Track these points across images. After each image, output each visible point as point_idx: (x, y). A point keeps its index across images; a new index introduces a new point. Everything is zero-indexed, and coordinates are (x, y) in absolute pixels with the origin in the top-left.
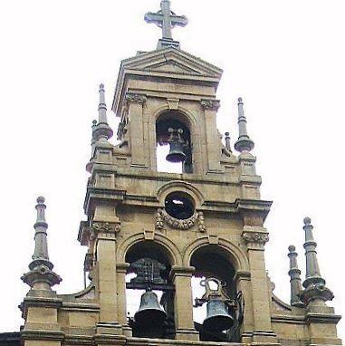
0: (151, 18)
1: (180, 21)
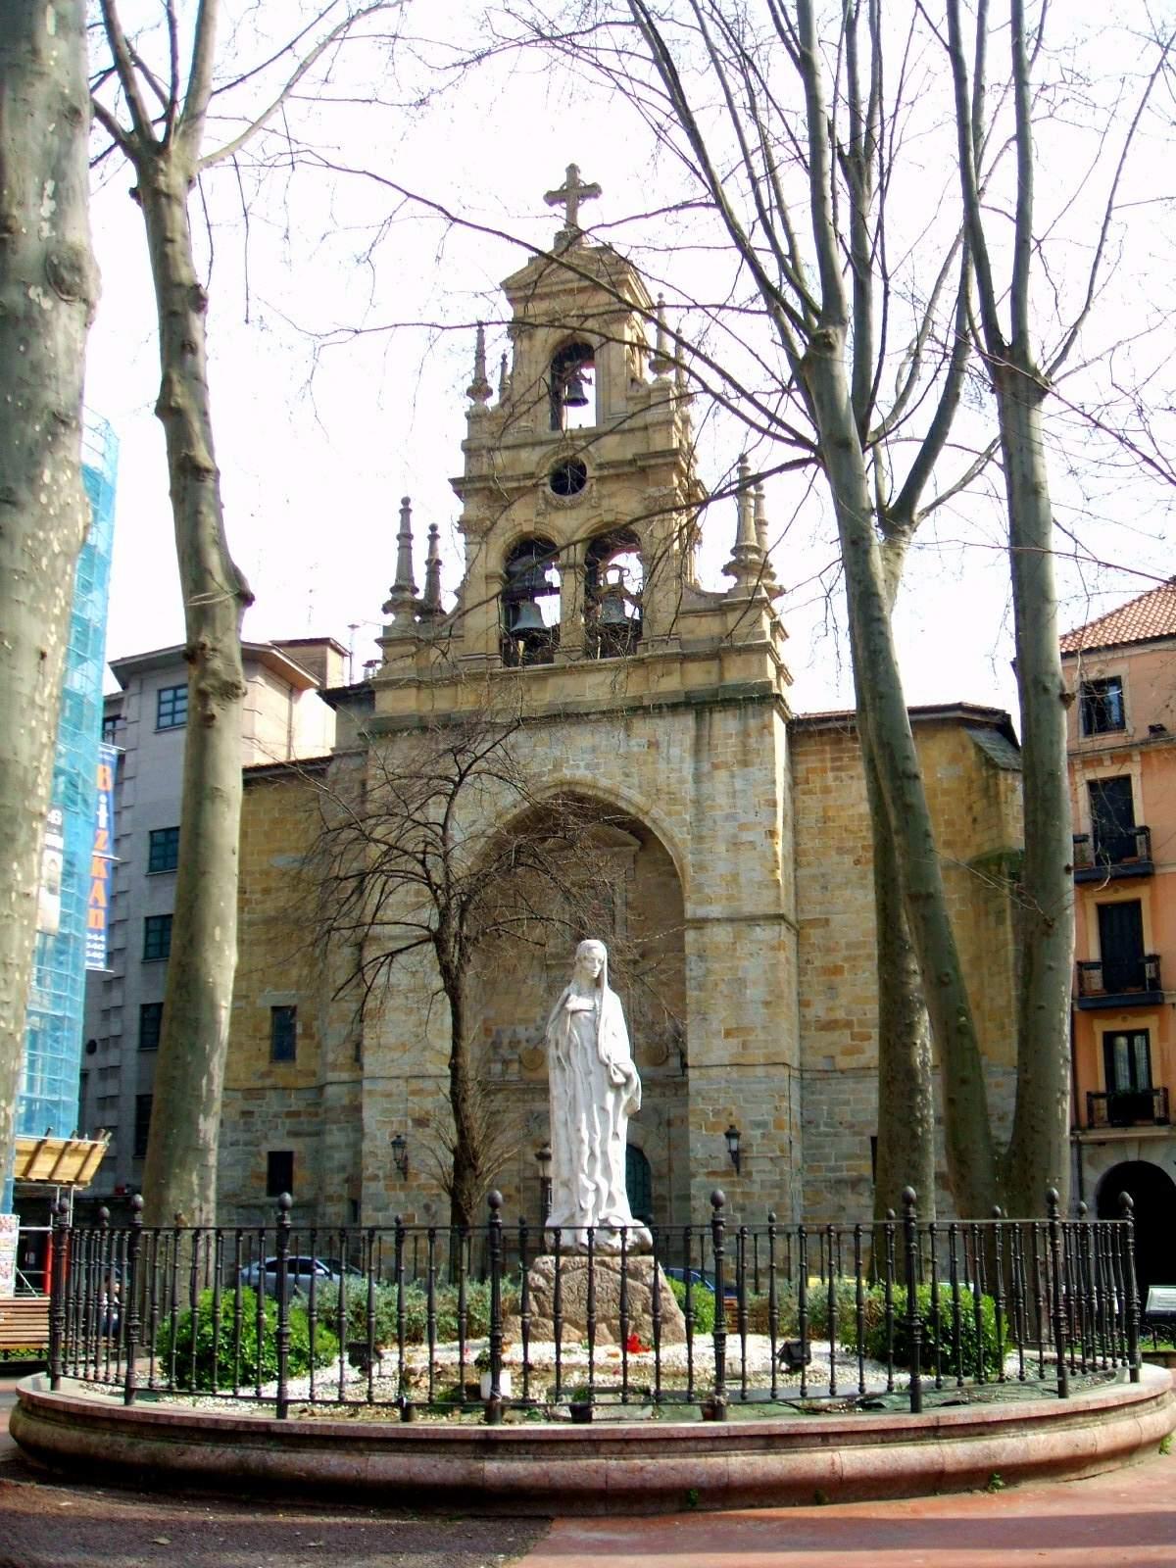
0: (552, 198)
1: (593, 191)
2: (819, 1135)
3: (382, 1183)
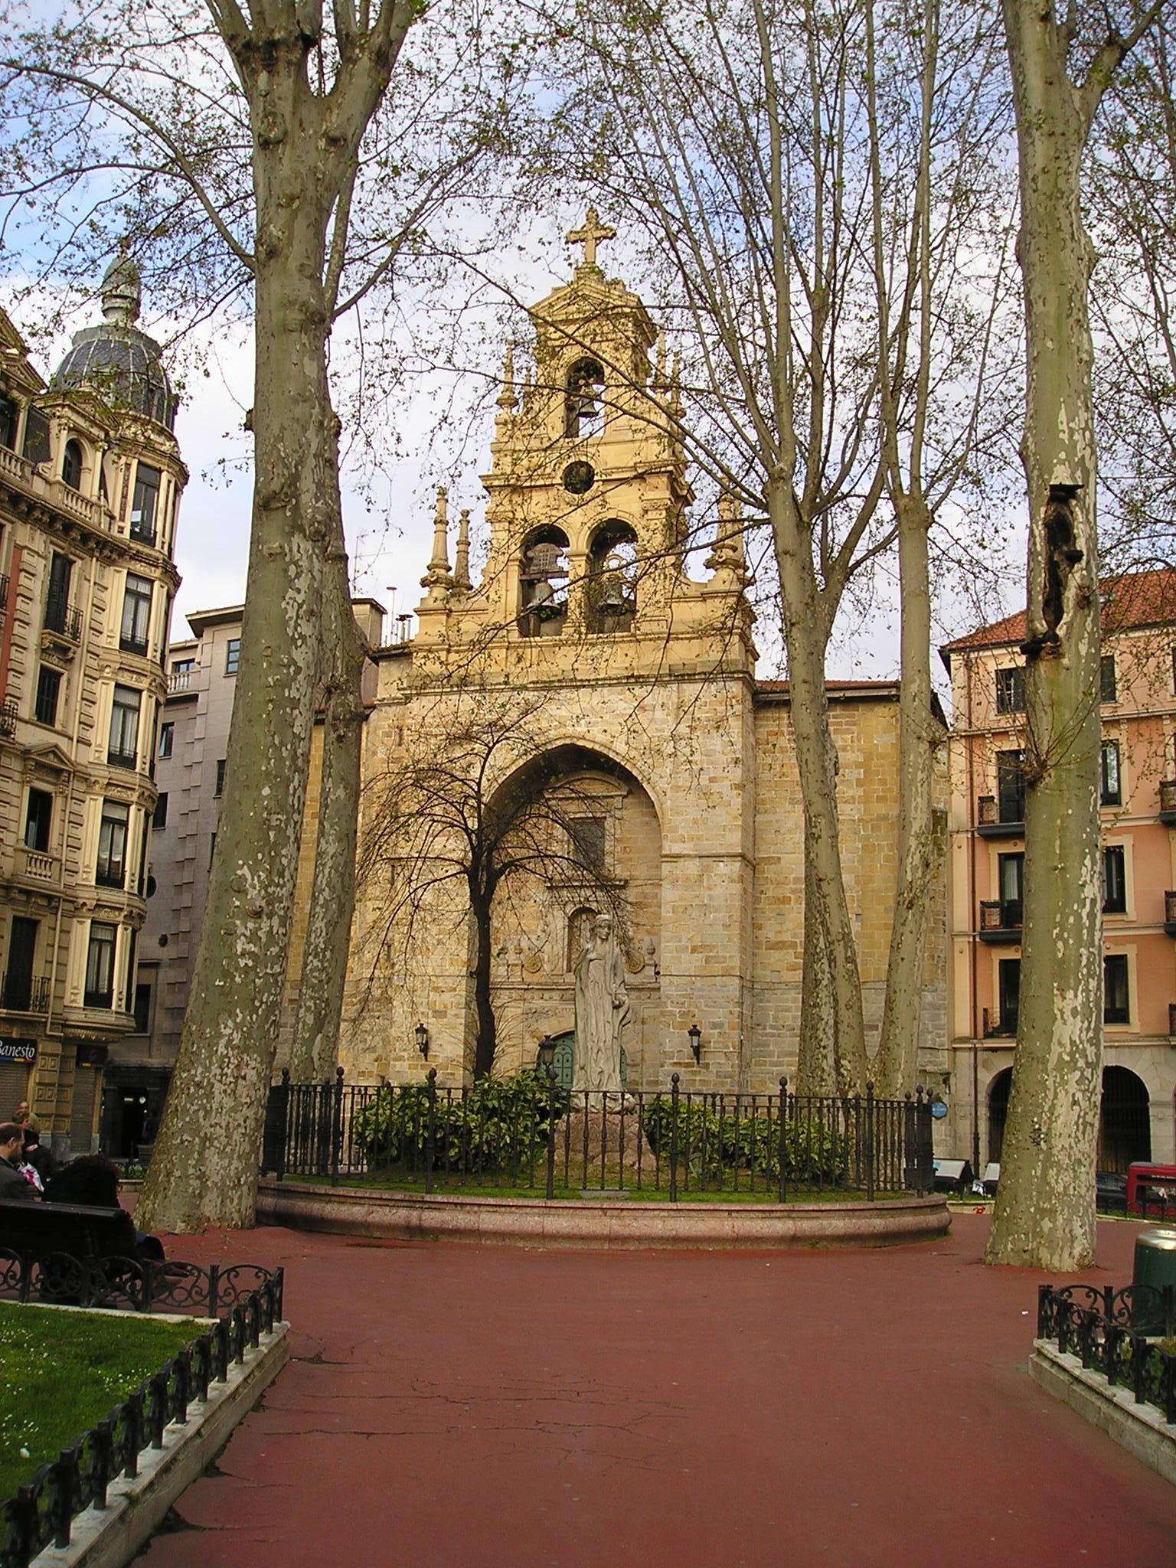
2: (766, 1035)
3: (406, 1063)
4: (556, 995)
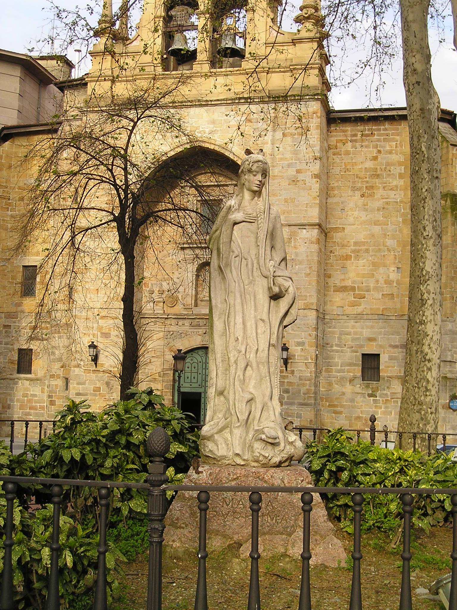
2: (333, 351)
4: (187, 323)
